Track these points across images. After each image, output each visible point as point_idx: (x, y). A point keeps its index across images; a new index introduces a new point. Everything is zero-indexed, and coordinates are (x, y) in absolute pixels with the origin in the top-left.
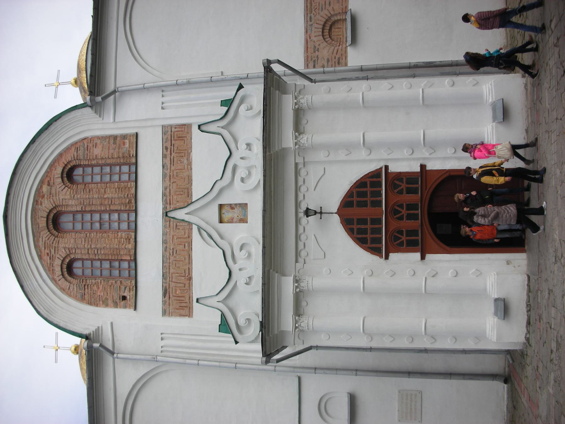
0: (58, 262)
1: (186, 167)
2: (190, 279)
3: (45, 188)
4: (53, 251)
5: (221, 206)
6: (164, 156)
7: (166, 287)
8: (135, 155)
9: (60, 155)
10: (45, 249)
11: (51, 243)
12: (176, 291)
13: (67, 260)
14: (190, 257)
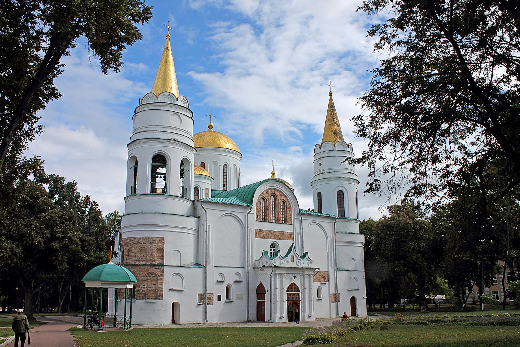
3: (281, 194)
4: (267, 194)
5: (294, 256)
6: (287, 232)
9: (288, 200)
14: (267, 238)
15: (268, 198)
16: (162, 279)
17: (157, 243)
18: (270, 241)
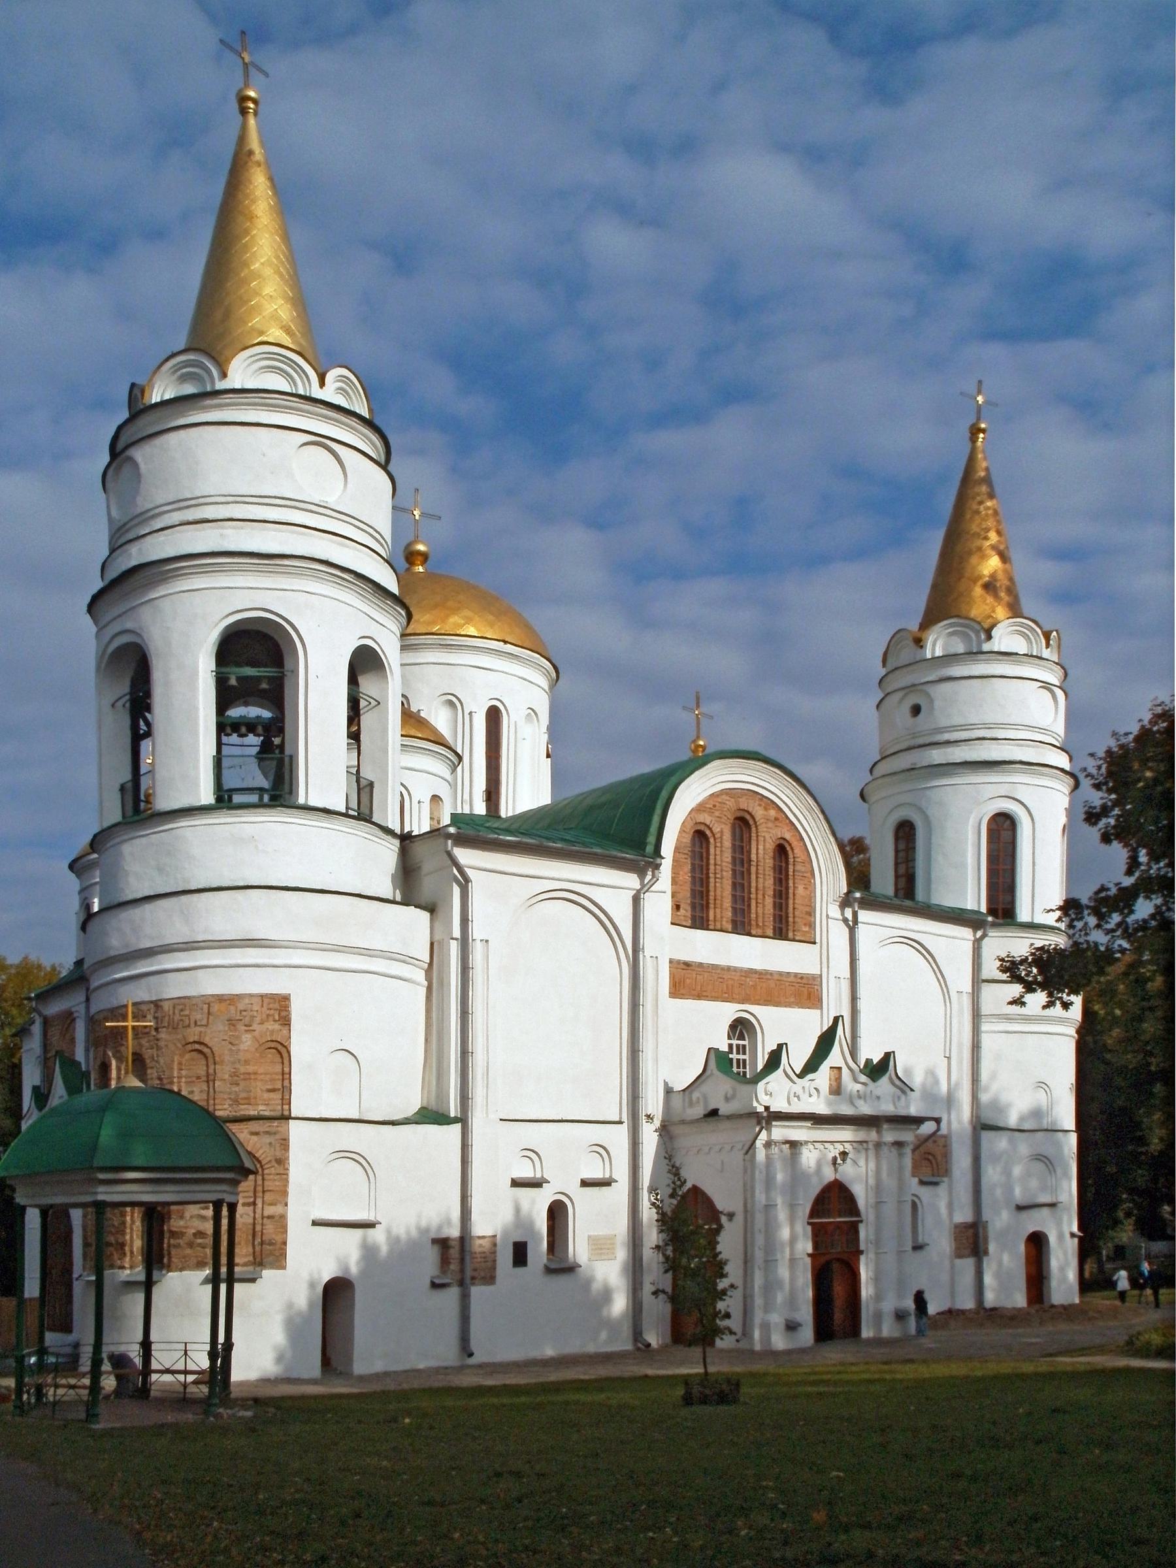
0: (706, 818)
1: (787, 1000)
2: (699, 997)
4: (717, 814)
6: (796, 975)
7: (692, 966)
8: (797, 938)
10: (720, 803)
11: (725, 813)
12: (689, 978)
13: (708, 832)
15: (722, 832)
16: (284, 1176)
17: (258, 1020)
18: (729, 1011)
